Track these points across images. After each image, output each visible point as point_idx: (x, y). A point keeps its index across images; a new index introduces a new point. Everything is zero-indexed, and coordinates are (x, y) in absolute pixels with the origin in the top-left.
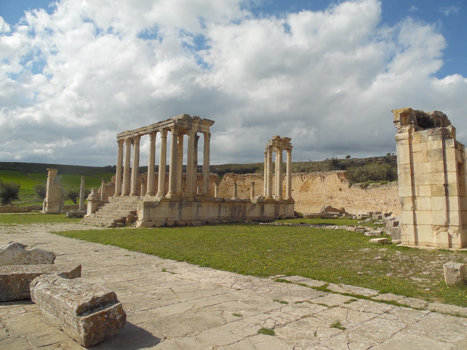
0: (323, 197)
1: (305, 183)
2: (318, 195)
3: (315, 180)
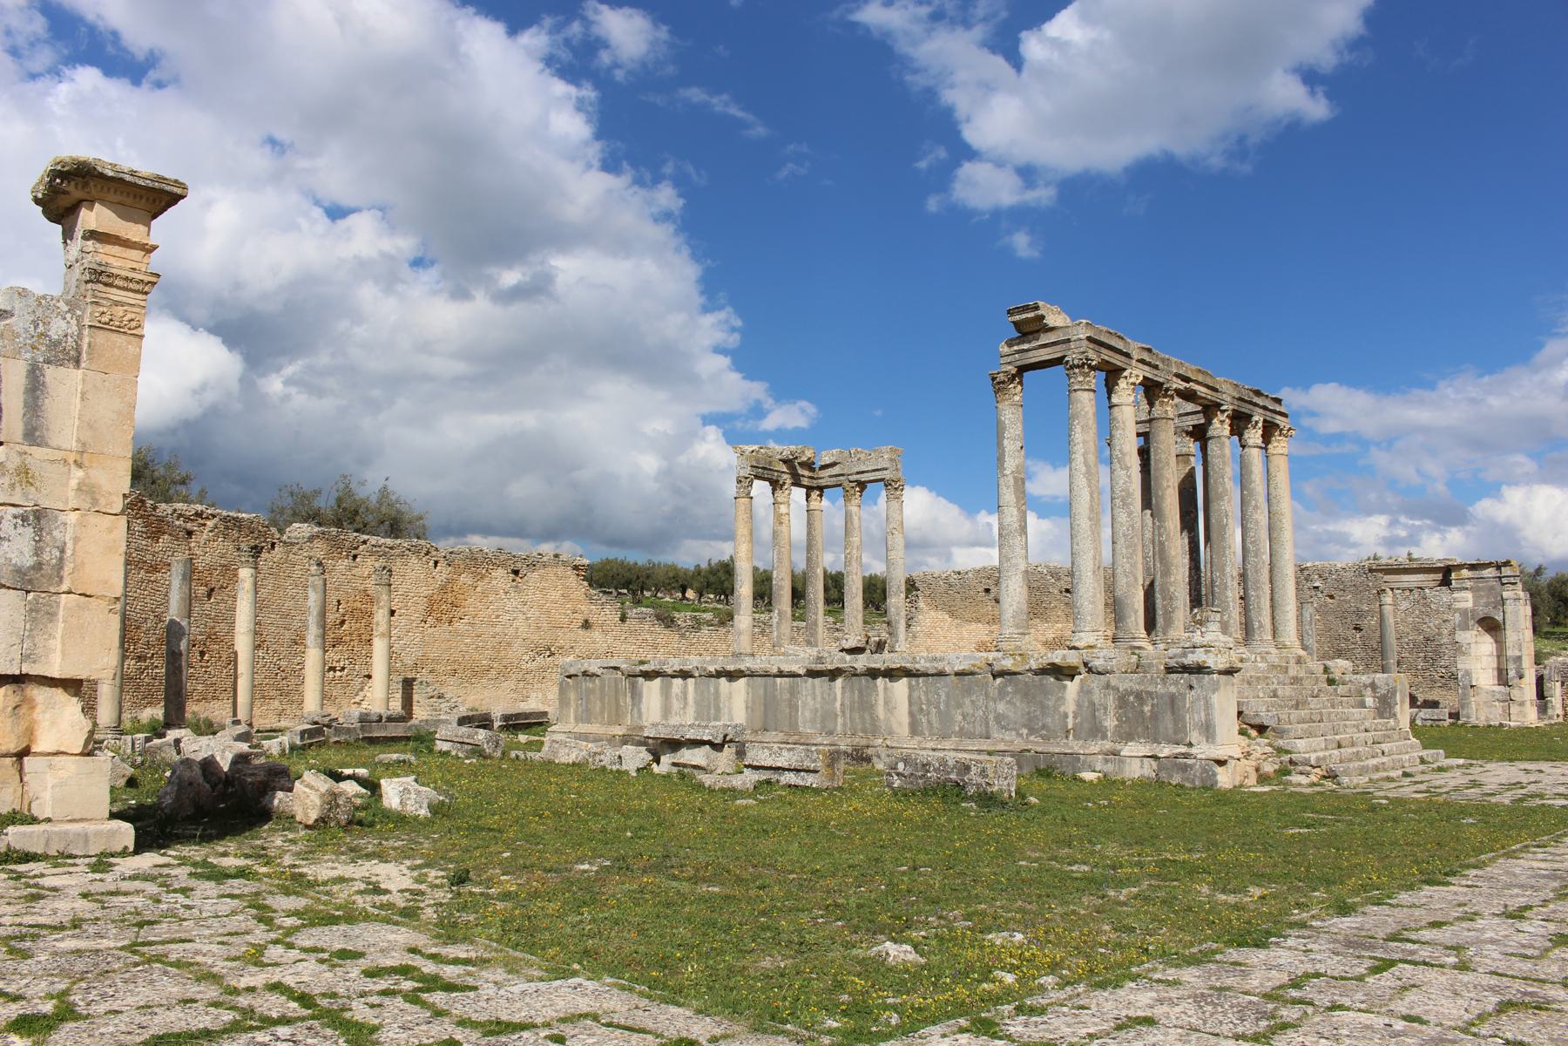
0: (517, 649)
1: (443, 589)
2: (497, 640)
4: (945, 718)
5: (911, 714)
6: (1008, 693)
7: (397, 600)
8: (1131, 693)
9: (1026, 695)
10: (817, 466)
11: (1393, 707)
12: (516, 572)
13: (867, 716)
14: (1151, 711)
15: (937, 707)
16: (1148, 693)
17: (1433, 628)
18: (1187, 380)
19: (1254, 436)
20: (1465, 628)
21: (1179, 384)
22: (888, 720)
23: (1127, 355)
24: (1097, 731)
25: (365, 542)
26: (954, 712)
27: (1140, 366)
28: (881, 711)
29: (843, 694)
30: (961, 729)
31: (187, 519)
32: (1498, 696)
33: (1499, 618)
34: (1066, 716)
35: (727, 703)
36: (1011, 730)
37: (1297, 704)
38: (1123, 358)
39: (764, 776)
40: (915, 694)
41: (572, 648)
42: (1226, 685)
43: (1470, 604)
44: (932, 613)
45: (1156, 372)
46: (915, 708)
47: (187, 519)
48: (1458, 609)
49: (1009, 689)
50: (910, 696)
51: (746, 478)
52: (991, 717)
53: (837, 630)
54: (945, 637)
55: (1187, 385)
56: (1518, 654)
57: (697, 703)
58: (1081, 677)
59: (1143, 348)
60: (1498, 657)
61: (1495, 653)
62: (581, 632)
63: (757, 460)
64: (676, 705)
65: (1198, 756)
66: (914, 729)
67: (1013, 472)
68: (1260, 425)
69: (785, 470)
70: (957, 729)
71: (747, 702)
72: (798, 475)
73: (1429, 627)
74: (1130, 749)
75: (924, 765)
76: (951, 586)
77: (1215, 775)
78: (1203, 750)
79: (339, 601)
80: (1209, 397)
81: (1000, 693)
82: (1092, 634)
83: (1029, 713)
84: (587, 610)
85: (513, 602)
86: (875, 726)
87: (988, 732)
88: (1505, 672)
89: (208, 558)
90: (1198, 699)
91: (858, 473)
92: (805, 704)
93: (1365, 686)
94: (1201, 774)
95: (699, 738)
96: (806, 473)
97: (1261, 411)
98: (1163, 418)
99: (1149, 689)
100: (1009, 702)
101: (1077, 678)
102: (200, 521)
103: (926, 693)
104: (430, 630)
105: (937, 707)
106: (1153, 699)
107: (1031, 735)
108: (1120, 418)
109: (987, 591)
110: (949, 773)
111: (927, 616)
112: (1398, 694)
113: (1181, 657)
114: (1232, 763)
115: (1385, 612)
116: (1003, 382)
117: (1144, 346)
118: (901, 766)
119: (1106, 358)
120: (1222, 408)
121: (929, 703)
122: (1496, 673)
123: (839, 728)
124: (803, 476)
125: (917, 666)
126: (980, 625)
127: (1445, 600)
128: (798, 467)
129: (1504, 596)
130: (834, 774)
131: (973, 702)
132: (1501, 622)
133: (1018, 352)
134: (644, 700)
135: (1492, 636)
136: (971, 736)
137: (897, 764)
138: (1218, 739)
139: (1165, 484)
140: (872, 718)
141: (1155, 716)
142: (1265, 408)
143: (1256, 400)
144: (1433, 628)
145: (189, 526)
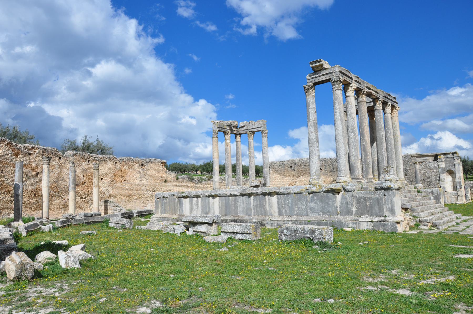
0: (143, 190)
1: (118, 171)
3: (133, 168)
4: (291, 209)
5: (279, 208)
6: (315, 200)
7: (103, 175)
8: (362, 198)
9: (322, 200)
10: (238, 127)
11: (440, 199)
12: (142, 165)
13: (262, 209)
14: (370, 205)
15: (288, 205)
16: (368, 198)
17: (429, 174)
18: (369, 89)
19: (388, 109)
20: (443, 173)
21: (367, 90)
22: (270, 210)
23: (352, 78)
24: (349, 212)
25: (92, 156)
26: (294, 207)
27: (356, 83)
28: (267, 207)
29: (253, 201)
30: (297, 213)
31: (29, 149)
32: (454, 194)
33: (453, 170)
34: (337, 207)
35: (212, 206)
36: (316, 213)
37: (414, 200)
38: (350, 80)
39: (230, 236)
40: (280, 201)
41: (161, 189)
42: (397, 194)
43: (444, 166)
44: (274, 174)
45: (360, 85)
46: (280, 206)
47: (29, 149)
48: (440, 168)
49: (315, 198)
50: (278, 202)
51: (216, 131)
52: (309, 208)
53: (245, 181)
54: (279, 182)
55: (370, 91)
56: (460, 181)
57: (202, 206)
58: (342, 193)
59: (356, 77)
60: (453, 182)
61: (452, 181)
62: (164, 183)
63: (219, 125)
64: (195, 207)
65: (390, 221)
66: (280, 213)
67: (313, 121)
68: (390, 106)
69: (228, 128)
70: (296, 213)
71: (219, 205)
72: (233, 130)
73: (428, 174)
74: (362, 219)
75: (295, 231)
76: (280, 166)
77: (396, 227)
78: (391, 218)
79: (83, 176)
80: (376, 95)
81: (311, 200)
82: (345, 177)
83: (323, 207)
84: (166, 176)
85: (142, 175)
86: (266, 213)
87: (307, 214)
88: (455, 187)
89: (36, 163)
90: (388, 200)
91: (252, 129)
92: (240, 205)
93: (429, 193)
94: (391, 227)
95: (203, 221)
96: (235, 129)
97: (390, 101)
98: (363, 102)
99: (369, 196)
100: (315, 203)
101: (341, 193)
102: (34, 150)
103: (284, 201)
104: (115, 185)
105: (288, 205)
106: (370, 200)
107: (324, 214)
108: (349, 101)
109: (291, 167)
110: (306, 234)
111: (273, 175)
112: (441, 195)
113: (381, 184)
114: (402, 222)
115: (417, 169)
116: (308, 89)
117: (356, 76)
118: (285, 231)
119: (345, 79)
120: (380, 99)
121: (285, 204)
122: (452, 187)
123: (253, 214)
124: (234, 130)
125: (280, 191)
126: (289, 178)
127: (433, 165)
128: (232, 128)
129: (455, 163)
130: (257, 234)
131: (301, 203)
132: (454, 171)
133: (313, 78)
134: (184, 206)
135: (451, 176)
136: (301, 215)
137: (283, 230)
138: (396, 214)
139: (364, 125)
140: (264, 210)
141: (371, 206)
142: (391, 100)
143: (389, 97)
144: (429, 174)
145: (30, 152)
